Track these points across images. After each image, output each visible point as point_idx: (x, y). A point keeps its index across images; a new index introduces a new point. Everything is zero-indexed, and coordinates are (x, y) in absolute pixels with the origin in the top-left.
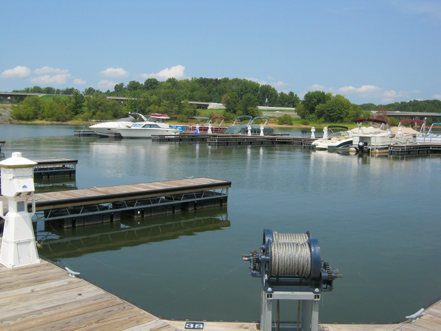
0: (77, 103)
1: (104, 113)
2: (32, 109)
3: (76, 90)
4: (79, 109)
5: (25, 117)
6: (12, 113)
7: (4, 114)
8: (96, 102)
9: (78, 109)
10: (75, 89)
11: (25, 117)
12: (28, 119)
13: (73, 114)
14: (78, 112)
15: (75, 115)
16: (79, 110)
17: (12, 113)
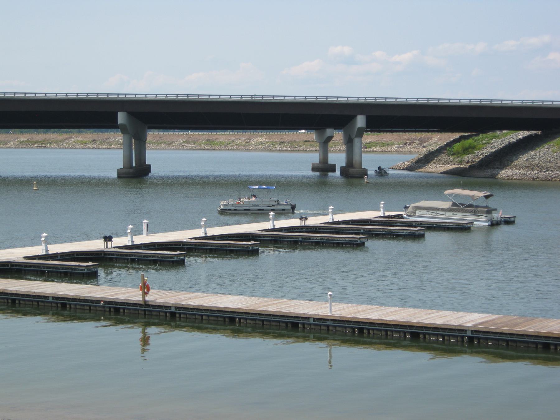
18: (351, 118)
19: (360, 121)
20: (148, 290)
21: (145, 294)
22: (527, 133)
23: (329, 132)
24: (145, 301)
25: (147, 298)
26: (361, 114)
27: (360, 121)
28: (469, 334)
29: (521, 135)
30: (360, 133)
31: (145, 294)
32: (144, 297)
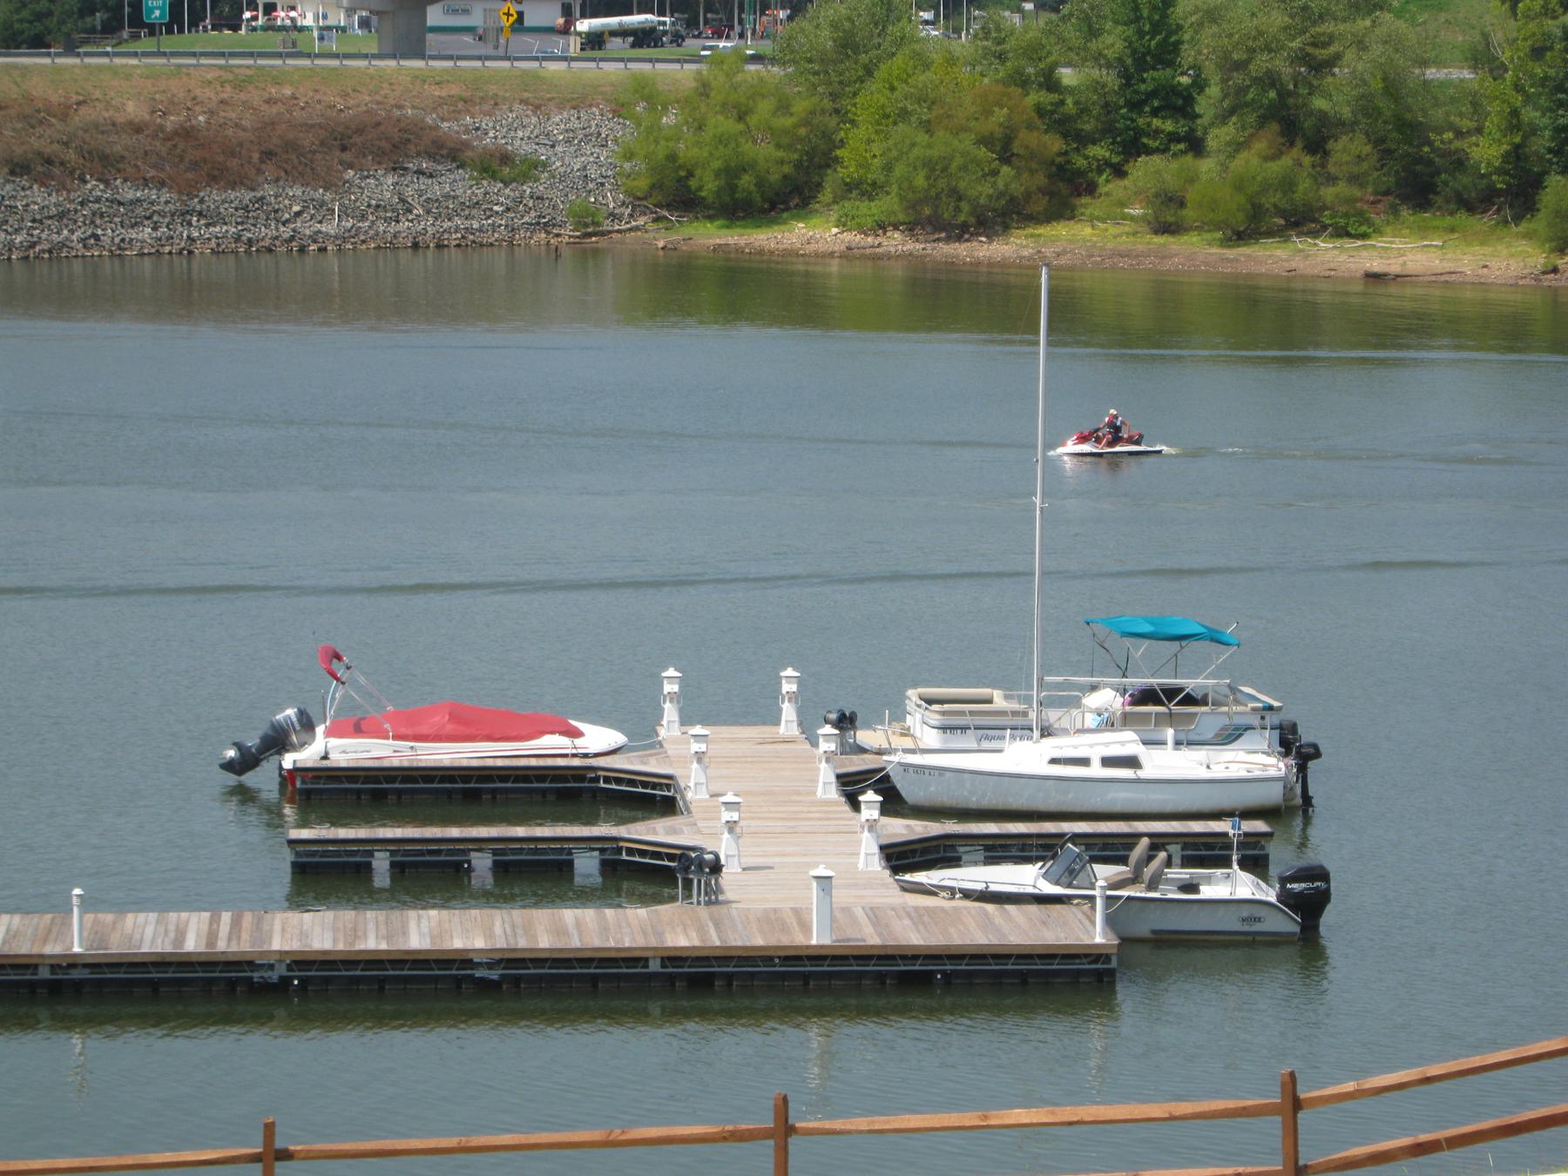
1: (1286, 161)
2: (788, 122)
4: (1155, 113)
5: (708, 185)
6: (629, 156)
7: (564, 160)
9: (1141, 121)
11: (708, 185)
12: (736, 209)
13: (1108, 164)
14: (1145, 145)
15: (1119, 172)
16: (1156, 122)
17: (629, 156)
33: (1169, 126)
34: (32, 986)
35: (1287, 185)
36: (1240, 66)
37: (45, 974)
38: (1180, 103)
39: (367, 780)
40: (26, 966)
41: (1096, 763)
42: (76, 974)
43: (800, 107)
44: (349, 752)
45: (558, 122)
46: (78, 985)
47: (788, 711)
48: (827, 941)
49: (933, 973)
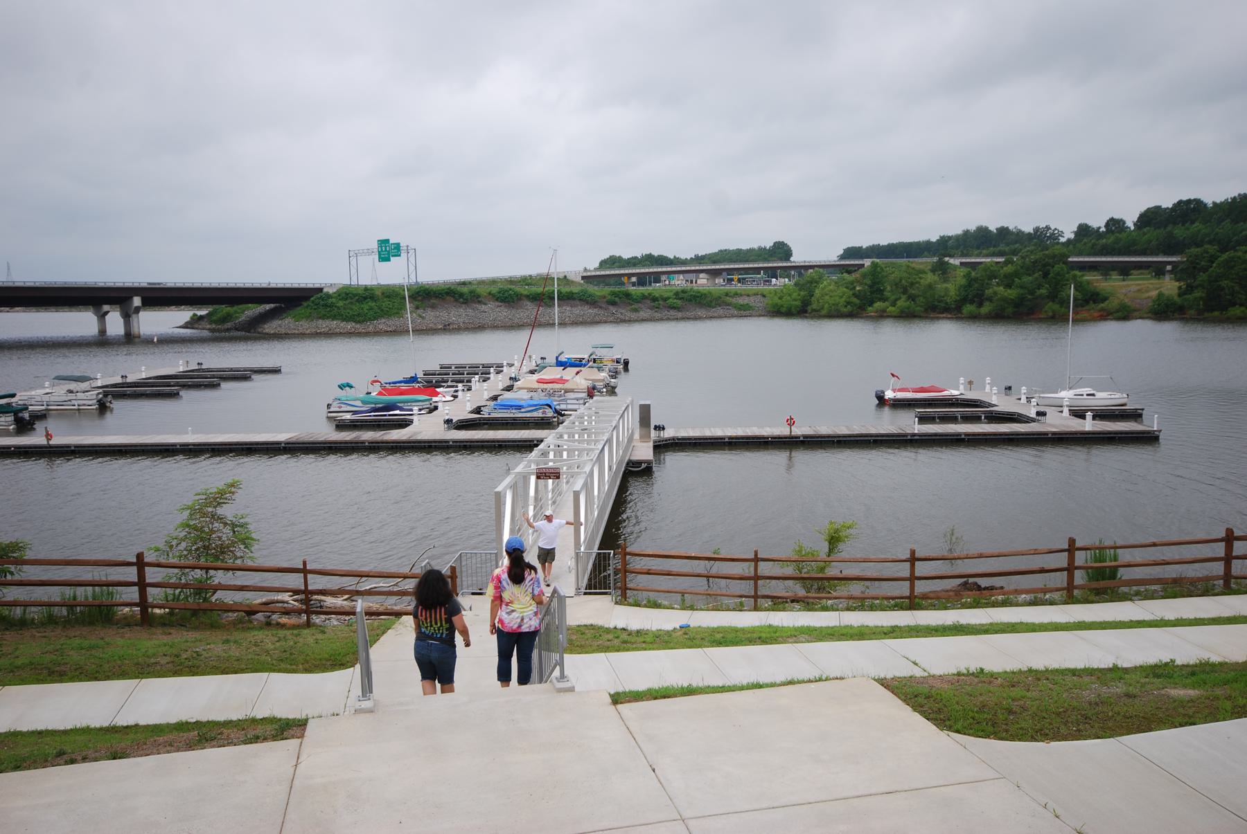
0: (874, 283)
1: (908, 303)
3: (1056, 229)
8: (901, 280)
10: (1053, 229)
18: (130, 298)
19: (137, 301)
20: (51, 437)
21: (48, 440)
22: (272, 306)
23: (106, 308)
24: (50, 445)
25: (51, 443)
26: (137, 295)
27: (137, 301)
28: (283, 445)
29: (268, 307)
30: (137, 310)
31: (48, 440)
32: (48, 442)
33: (879, 296)
34: (906, 441)
35: (909, 308)
36: (896, 284)
37: (909, 437)
38: (881, 291)
39: (907, 401)
40: (904, 436)
41: (1085, 395)
42: (916, 438)
43: (802, 293)
44: (900, 395)
45: (752, 299)
46: (917, 440)
47: (988, 387)
48: (1090, 429)
49: (1115, 437)
